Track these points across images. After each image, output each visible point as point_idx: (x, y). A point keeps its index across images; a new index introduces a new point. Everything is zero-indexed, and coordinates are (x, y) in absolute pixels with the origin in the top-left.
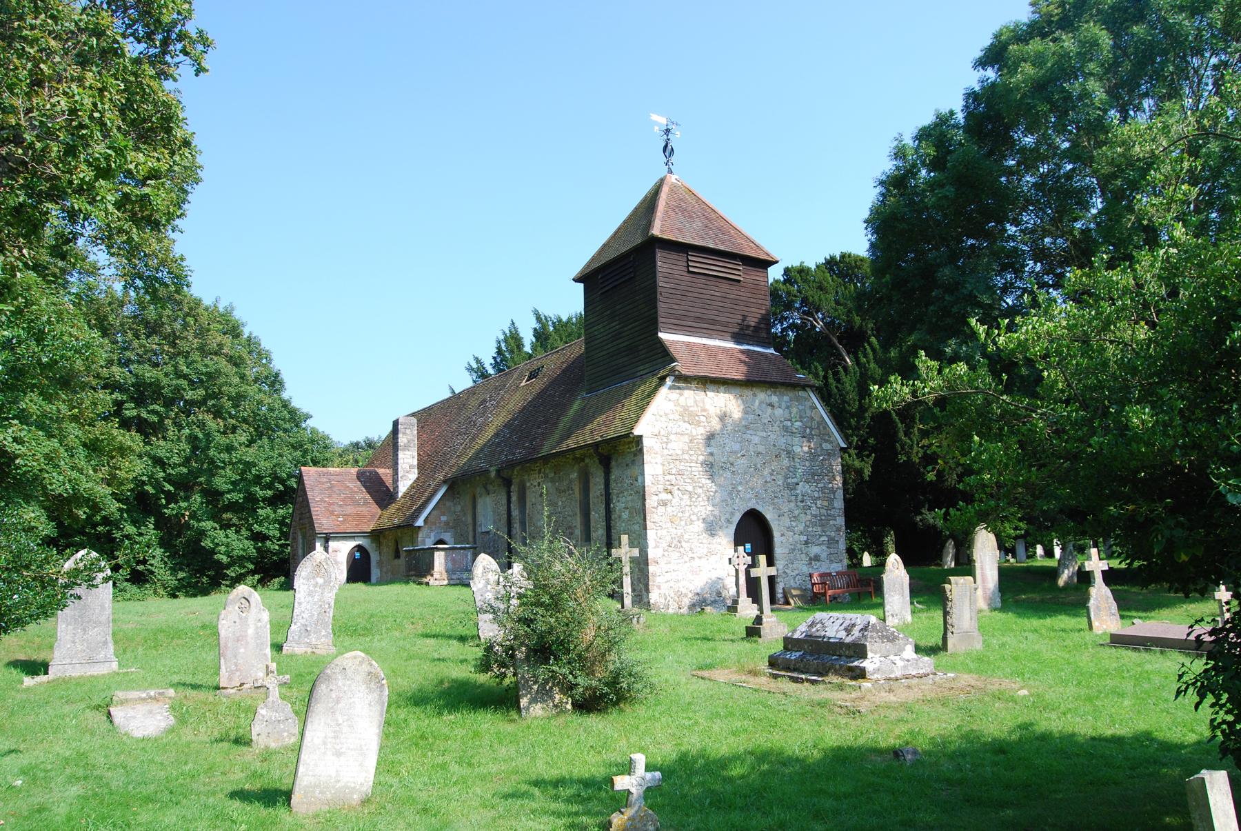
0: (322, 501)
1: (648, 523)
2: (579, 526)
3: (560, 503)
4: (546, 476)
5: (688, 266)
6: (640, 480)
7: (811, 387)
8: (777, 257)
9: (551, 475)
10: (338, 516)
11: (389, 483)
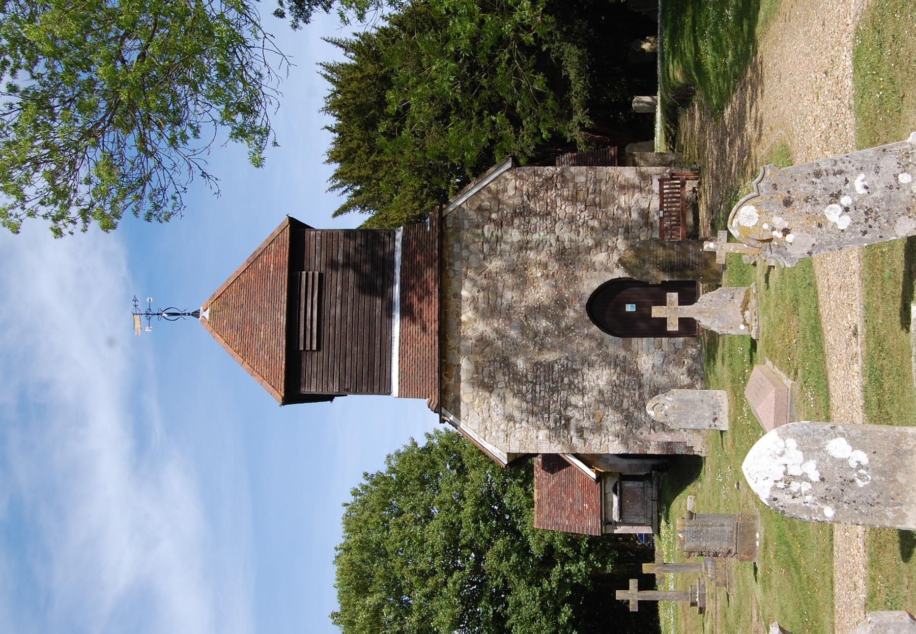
0: (568, 518)
10: (583, 507)
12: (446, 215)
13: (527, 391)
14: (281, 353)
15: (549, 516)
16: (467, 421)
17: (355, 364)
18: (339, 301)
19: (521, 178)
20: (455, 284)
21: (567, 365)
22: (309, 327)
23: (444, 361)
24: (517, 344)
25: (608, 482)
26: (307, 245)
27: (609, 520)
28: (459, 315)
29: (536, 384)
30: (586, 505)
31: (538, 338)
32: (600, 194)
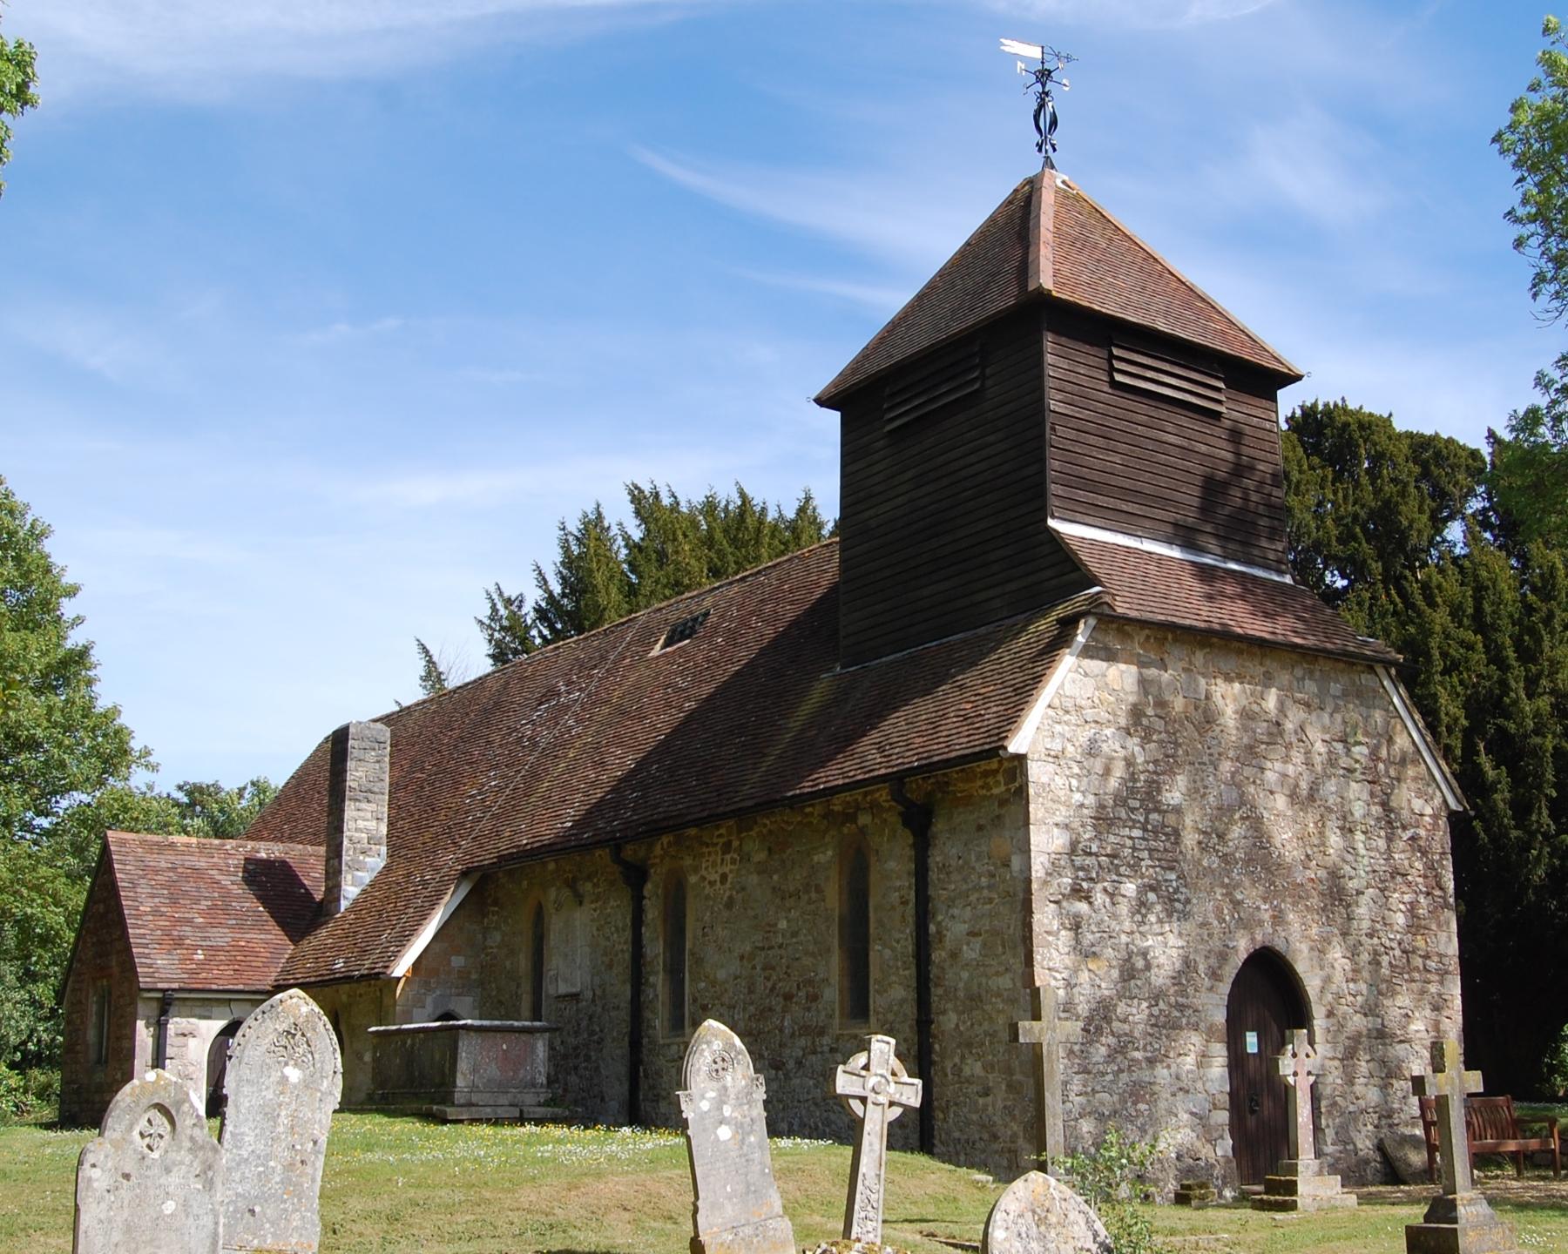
0: (156, 912)
1: (1037, 969)
2: (835, 978)
3: (783, 924)
4: (745, 858)
5: (1112, 369)
6: (1016, 862)
7: (1387, 664)
8: (1299, 368)
9: (761, 856)
11: (313, 880)
12: (1377, 675)
13: (1133, 810)
14: (1111, 309)
15: (149, 871)
16: (1077, 671)
17: (1094, 454)
18: (1185, 443)
19: (1435, 825)
20: (1285, 677)
21: (1178, 900)
22: (1150, 374)
23: (1170, 637)
24: (1205, 794)
26: (1257, 401)
27: (172, 1010)
28: (1241, 678)
29: (1145, 830)
30: (200, 956)
31: (1216, 840)
32: (1425, 982)
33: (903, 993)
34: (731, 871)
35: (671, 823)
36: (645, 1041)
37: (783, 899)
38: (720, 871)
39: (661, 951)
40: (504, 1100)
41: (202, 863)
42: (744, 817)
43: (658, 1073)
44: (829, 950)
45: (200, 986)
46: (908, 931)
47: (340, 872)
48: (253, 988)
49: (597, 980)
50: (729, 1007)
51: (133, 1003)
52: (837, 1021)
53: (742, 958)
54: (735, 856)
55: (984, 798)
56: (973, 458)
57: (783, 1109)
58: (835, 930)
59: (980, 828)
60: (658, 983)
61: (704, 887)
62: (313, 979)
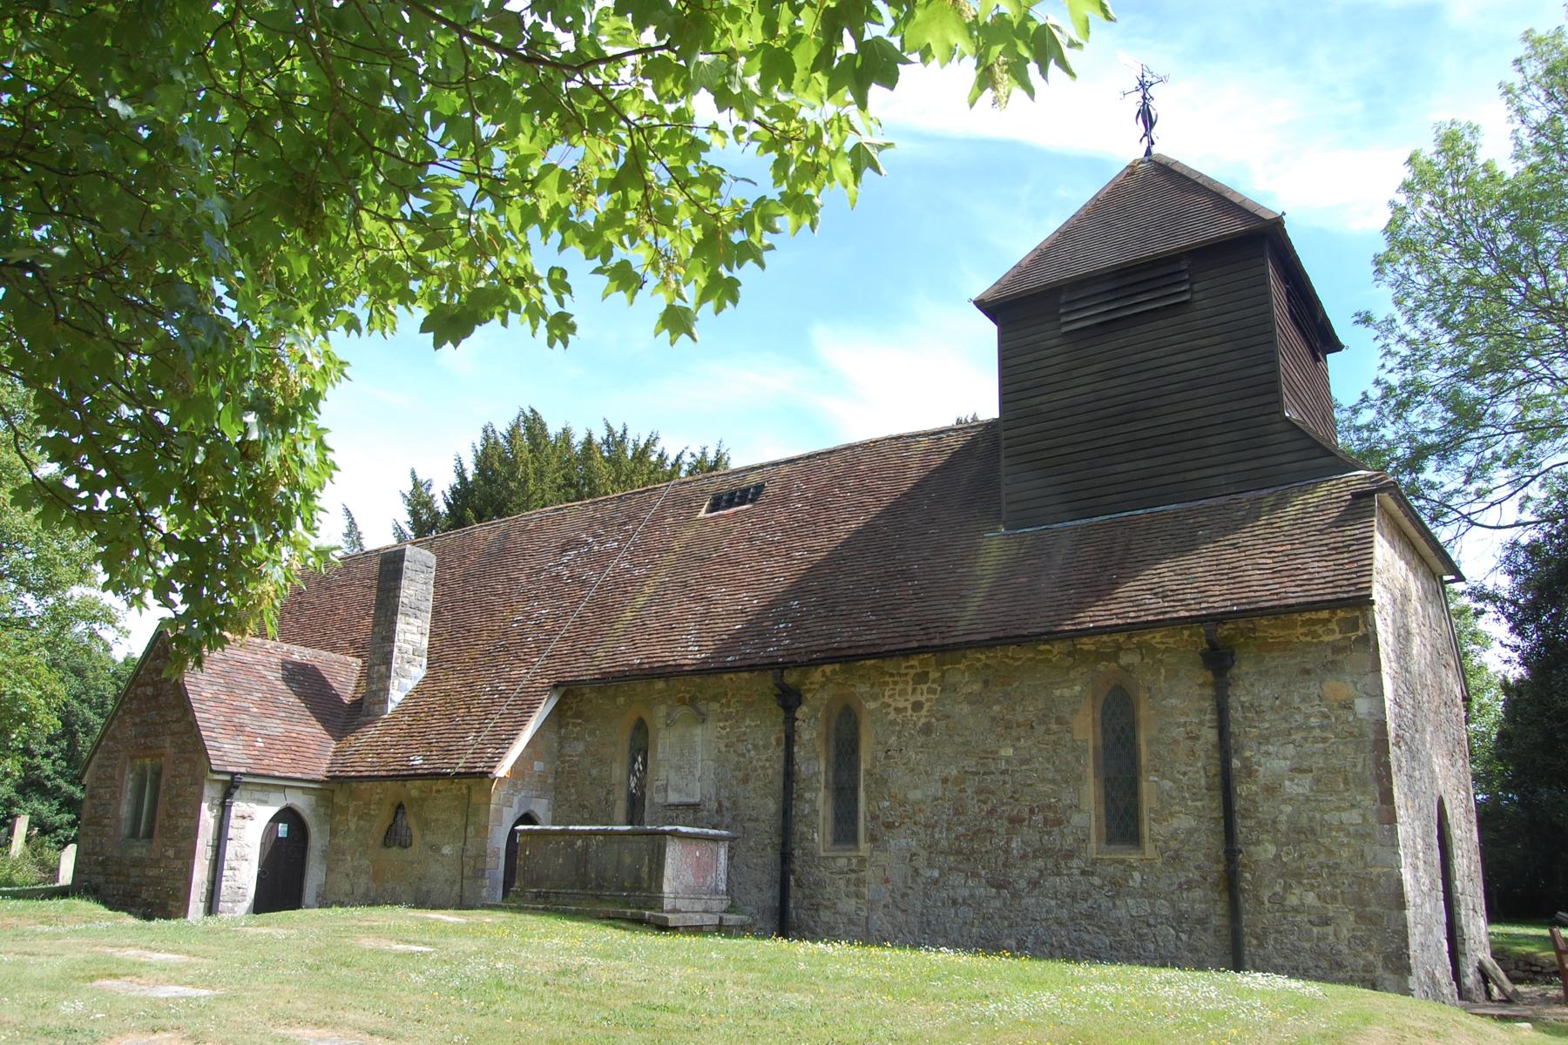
0: (215, 698)
4: (948, 689)
10: (255, 735)
25: (305, 797)
27: (237, 794)
33: (1194, 823)
34: (927, 700)
35: (860, 651)
36: (797, 852)
37: (1008, 727)
38: (912, 699)
39: (822, 768)
40: (699, 906)
41: (249, 658)
42: (947, 651)
43: (819, 884)
44: (1079, 778)
45: (265, 772)
46: (1199, 765)
47: (389, 677)
48: (309, 777)
49: (724, 793)
50: (925, 826)
51: (198, 783)
52: (1093, 845)
53: (945, 781)
54: (935, 686)
55: (1309, 644)
56: (1181, 357)
57: (1010, 926)
58: (1089, 760)
59: (1307, 672)
60: (818, 802)
61: (888, 714)
62: (384, 773)
